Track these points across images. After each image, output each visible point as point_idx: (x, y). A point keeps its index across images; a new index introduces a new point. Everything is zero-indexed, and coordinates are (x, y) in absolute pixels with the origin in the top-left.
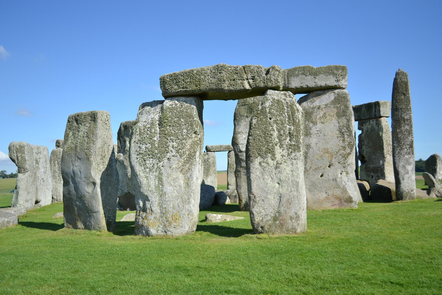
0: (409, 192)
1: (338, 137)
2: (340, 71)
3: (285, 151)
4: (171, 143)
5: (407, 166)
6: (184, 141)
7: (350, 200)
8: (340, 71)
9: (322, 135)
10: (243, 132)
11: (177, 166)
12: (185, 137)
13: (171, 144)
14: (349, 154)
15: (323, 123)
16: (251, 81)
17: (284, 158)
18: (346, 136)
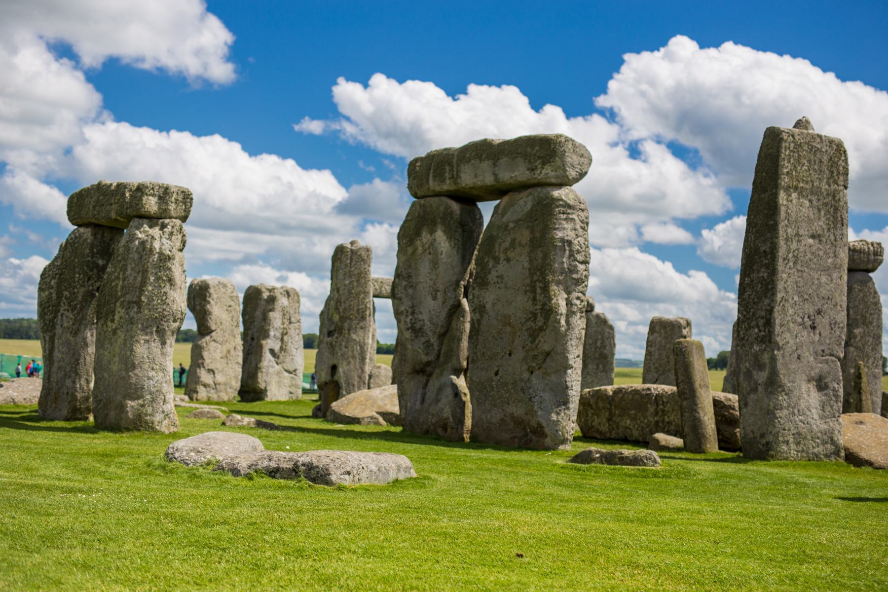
0: (755, 438)
1: (526, 291)
2: (537, 148)
5: (755, 372)
6: (76, 290)
8: (537, 148)
14: (541, 329)
15: (508, 260)
18: (539, 291)
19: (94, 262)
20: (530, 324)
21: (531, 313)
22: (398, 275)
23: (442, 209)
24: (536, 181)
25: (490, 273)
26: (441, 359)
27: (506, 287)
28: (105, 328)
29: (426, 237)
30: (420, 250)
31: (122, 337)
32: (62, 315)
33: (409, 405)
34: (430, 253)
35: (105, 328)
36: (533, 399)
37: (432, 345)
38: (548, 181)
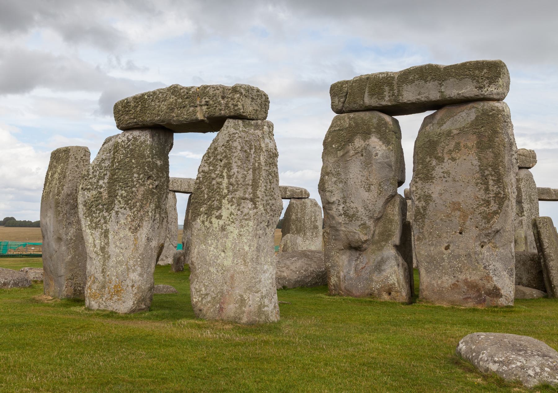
1: (477, 184)
3: (234, 207)
4: (120, 191)
6: (134, 189)
7: (496, 293)
8: (485, 71)
9: (449, 179)
10: (334, 172)
11: (125, 222)
12: (135, 183)
13: (120, 192)
14: (496, 213)
15: (453, 159)
16: (204, 108)
17: (232, 216)
18: (491, 182)
19: (154, 163)
20: (482, 209)
21: (483, 200)
22: (325, 173)
23: (375, 121)
24: (482, 97)
25: (433, 169)
26: (376, 238)
27: (454, 180)
28: (207, 223)
29: (358, 143)
30: (352, 152)
31: (236, 232)
32: (117, 213)
33: (342, 274)
34: (362, 155)
35: (207, 223)
36: (487, 268)
37: (369, 227)
38: (491, 96)
